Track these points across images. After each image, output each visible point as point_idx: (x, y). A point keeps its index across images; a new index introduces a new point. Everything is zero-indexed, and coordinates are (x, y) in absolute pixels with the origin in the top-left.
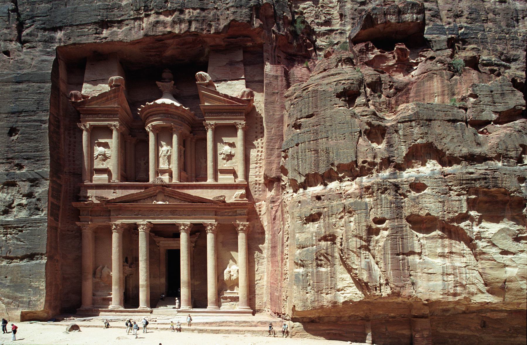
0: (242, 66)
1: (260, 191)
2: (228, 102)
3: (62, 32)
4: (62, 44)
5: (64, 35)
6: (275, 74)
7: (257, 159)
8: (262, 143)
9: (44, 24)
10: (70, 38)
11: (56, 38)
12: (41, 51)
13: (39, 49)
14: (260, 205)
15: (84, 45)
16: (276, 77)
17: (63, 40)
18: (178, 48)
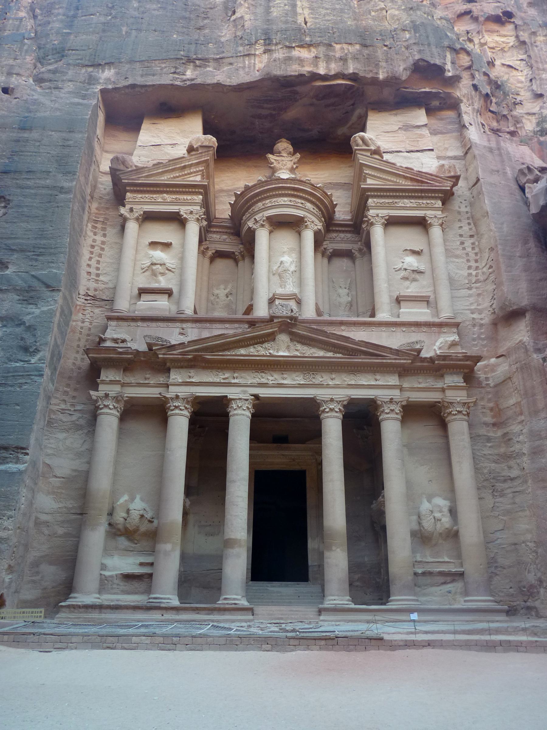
0: (425, 132)
1: (483, 339)
2: (412, 179)
3: (113, 71)
4: (110, 87)
5: (117, 74)
6: (486, 144)
7: (470, 281)
8: (476, 254)
9: (81, 59)
10: (126, 78)
11: (100, 78)
12: (69, 92)
13: (66, 90)
14: (486, 366)
15: (151, 89)
16: (491, 150)
17: (112, 80)
18: (312, 105)
